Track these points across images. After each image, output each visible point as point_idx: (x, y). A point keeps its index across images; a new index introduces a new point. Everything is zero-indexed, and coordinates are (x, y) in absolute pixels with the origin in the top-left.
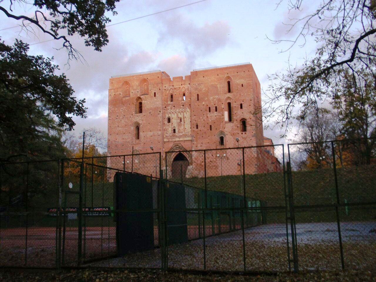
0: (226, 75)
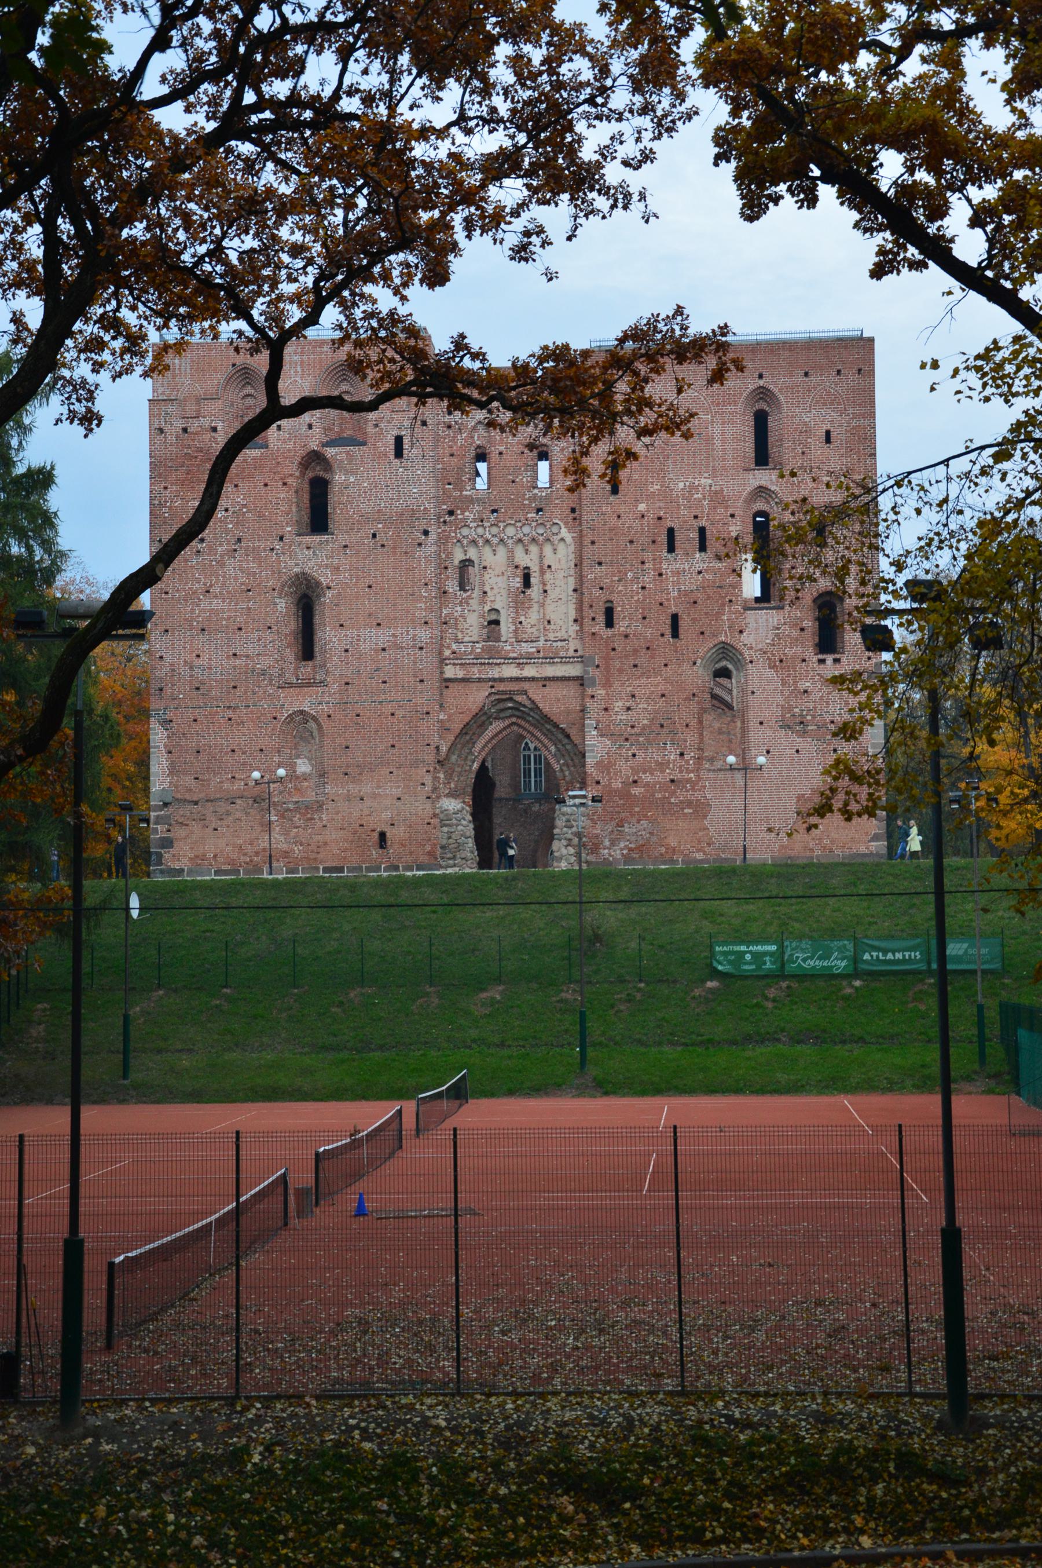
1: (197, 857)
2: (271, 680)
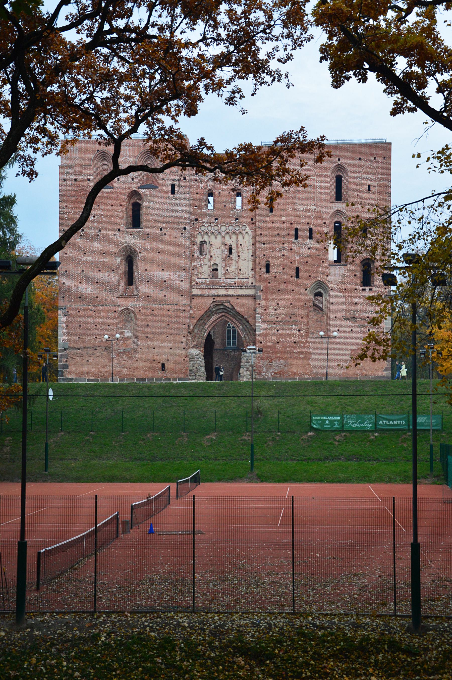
1: (79, 373)
2: (113, 294)
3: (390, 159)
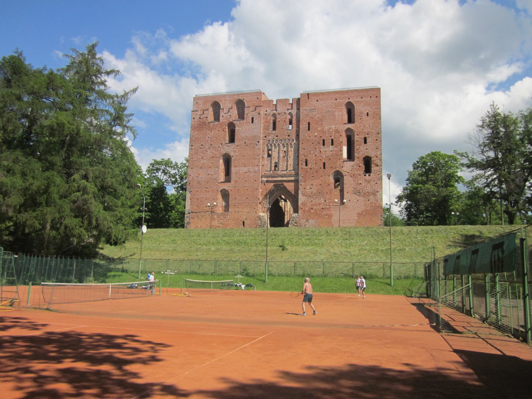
0: (347, 101)
3: (380, 97)
